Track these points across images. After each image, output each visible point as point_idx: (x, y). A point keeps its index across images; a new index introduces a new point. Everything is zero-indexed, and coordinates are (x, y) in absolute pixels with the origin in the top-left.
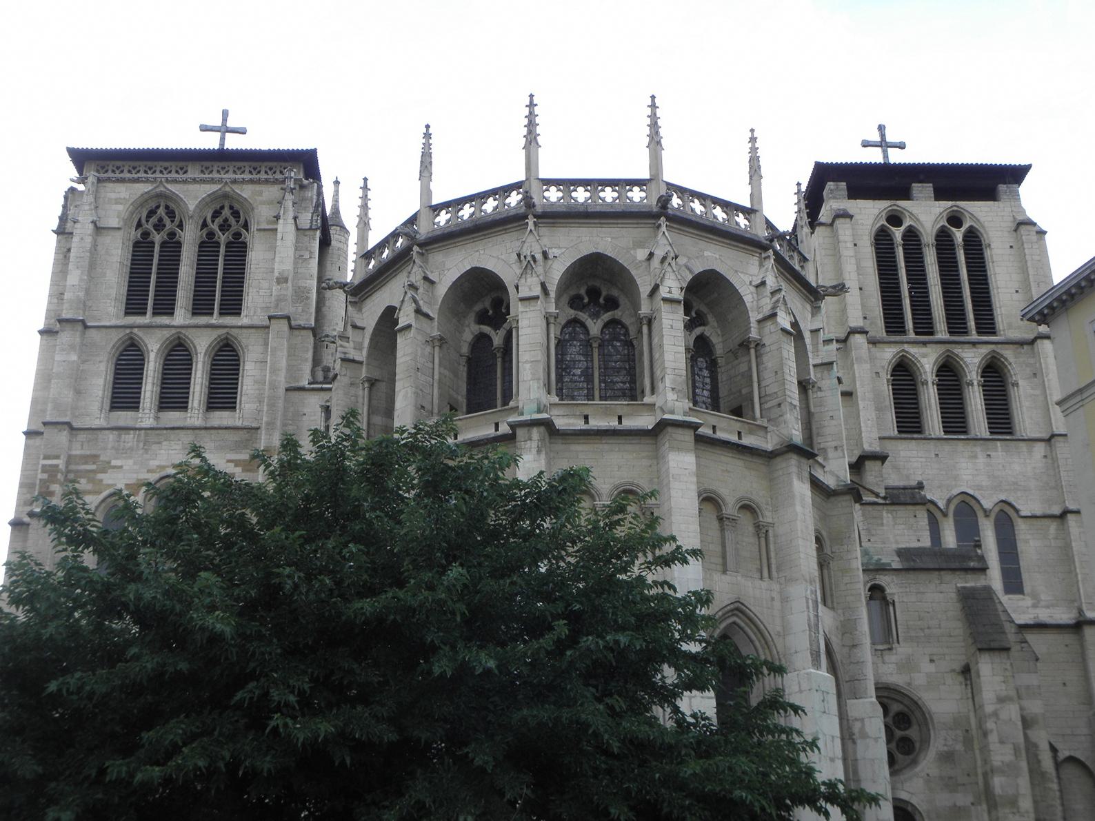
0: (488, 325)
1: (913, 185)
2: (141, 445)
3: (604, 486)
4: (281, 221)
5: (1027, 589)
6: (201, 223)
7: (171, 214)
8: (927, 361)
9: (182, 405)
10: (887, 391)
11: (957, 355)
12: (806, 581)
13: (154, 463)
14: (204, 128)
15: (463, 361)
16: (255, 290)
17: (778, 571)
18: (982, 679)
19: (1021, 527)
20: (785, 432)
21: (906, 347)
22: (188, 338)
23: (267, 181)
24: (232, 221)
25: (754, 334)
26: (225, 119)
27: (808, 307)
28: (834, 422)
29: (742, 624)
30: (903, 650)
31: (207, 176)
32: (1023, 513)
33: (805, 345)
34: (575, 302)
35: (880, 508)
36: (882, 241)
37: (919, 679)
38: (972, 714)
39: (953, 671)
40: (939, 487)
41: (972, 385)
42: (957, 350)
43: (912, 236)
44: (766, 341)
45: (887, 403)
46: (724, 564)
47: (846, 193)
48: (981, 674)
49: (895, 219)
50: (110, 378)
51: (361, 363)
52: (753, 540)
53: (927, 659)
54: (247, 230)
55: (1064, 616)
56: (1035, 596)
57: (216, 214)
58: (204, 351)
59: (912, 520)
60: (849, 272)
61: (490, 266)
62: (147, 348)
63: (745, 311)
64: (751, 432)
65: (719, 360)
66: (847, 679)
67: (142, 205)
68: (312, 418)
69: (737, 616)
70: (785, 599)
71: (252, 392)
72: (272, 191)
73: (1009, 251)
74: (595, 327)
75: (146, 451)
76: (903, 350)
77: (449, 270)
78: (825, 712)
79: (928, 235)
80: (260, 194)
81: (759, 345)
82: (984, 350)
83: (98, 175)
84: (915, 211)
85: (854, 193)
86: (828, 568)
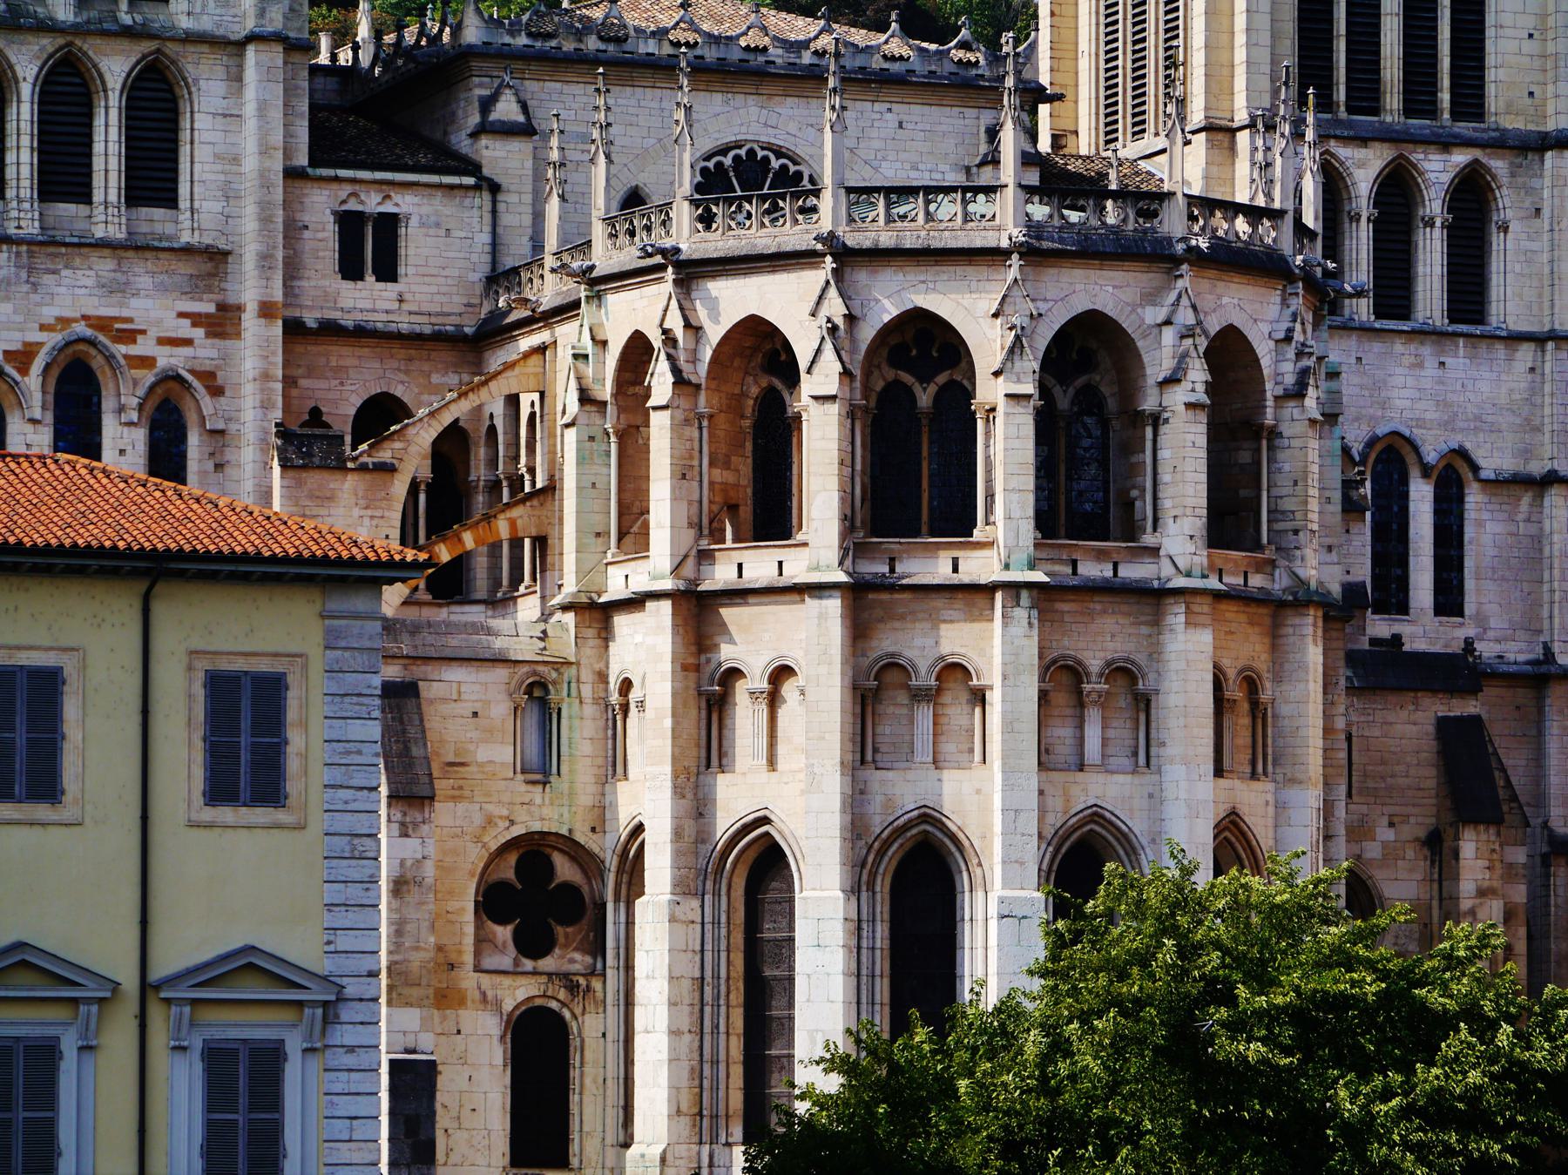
0: (908, 371)
2: (24, 275)
3: (1093, 662)
5: (1469, 608)
9: (83, 194)
11: (1415, 166)
13: (49, 313)
17: (1274, 765)
18: (1462, 863)
19: (1474, 498)
20: (1301, 572)
22: (85, 54)
25: (1269, 420)
29: (1233, 839)
32: (1484, 474)
38: (1435, 903)
39: (1417, 839)
41: (1432, 225)
42: (1417, 156)
44: (1286, 429)
48: (1461, 856)
51: (698, 387)
52: (1246, 721)
53: (1385, 821)
55: (1518, 652)
56: (1481, 620)
58: (118, 86)
62: (14, 72)
68: (320, 235)
70: (1280, 807)
71: (213, 177)
74: (1063, 401)
75: (35, 287)
81: (1274, 433)
82: (1460, 158)
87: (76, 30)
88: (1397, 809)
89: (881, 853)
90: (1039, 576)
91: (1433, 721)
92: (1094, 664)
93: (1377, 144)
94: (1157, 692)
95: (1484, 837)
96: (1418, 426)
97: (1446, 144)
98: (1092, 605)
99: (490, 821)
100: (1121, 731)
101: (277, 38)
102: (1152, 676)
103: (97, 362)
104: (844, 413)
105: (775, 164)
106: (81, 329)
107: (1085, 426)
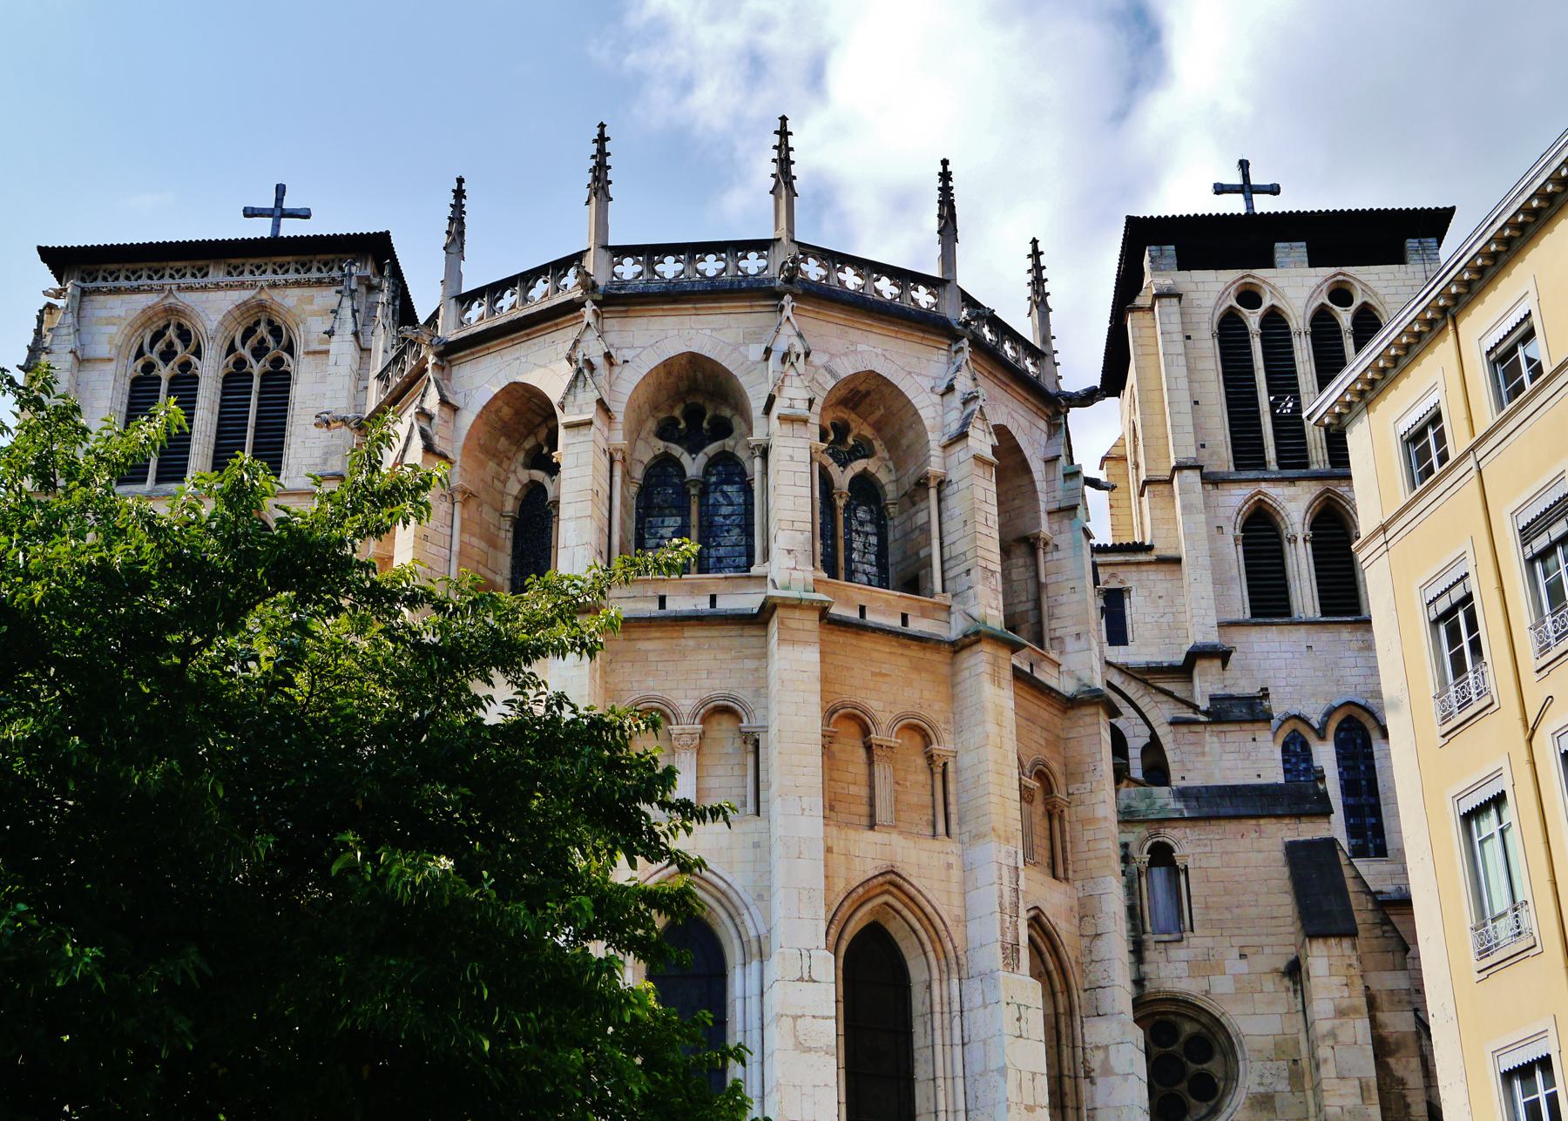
1: (1277, 245)
3: (683, 702)
4: (334, 338)
6: (226, 347)
7: (184, 335)
10: (1234, 556)
11: (1341, 497)
12: (999, 837)
14: (250, 213)
15: (506, 524)
16: (298, 441)
17: (960, 824)
20: (976, 612)
21: (1264, 487)
23: (319, 282)
26: (279, 199)
27: (1043, 425)
28: (1076, 597)
29: (899, 906)
30: (1197, 942)
31: (235, 278)
33: (1033, 482)
34: (666, 431)
35: (1200, 728)
36: (1230, 331)
37: (1222, 985)
38: (1302, 1037)
39: (1276, 970)
40: (1313, 695)
43: (1275, 322)
44: (953, 476)
45: (1235, 572)
46: (872, 816)
49: (1250, 297)
52: (923, 777)
53: (1235, 953)
54: (292, 355)
57: (248, 333)
59: (1250, 745)
60: (1176, 378)
61: (533, 379)
63: (922, 434)
64: (924, 613)
65: (891, 509)
66: (1086, 987)
67: (144, 326)
69: (890, 893)
70: (967, 869)
72: (328, 297)
74: (693, 466)
76: (1260, 492)
77: (477, 388)
78: (1021, 1036)
79: (1299, 319)
80: (311, 300)
83: (83, 285)
84: (1278, 283)
86: (1061, 819)
88: (1250, 941)
91: (1282, 848)
92: (686, 701)
93: (1304, 483)
94: (765, 729)
95: (1336, 951)
96: (1372, 697)
98: (683, 642)
102: (759, 713)
107: (724, 494)
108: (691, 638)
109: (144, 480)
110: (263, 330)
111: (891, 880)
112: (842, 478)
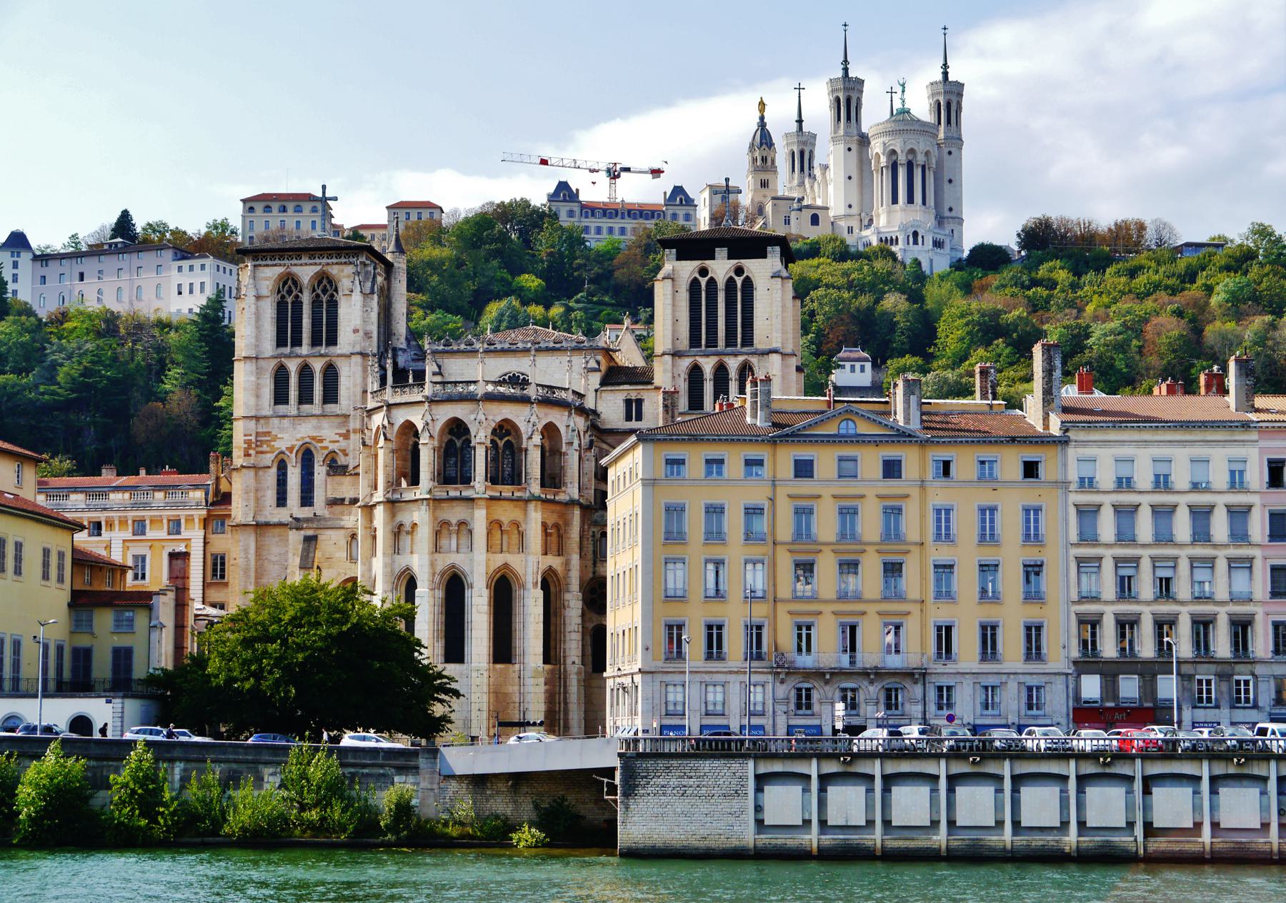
7: (295, 283)
8: (708, 365)
13: (299, 436)
21: (697, 358)
23: (345, 263)
24: (328, 286)
25: (524, 446)
26: (324, 193)
43: (712, 282)
47: (674, 256)
49: (704, 272)
50: (273, 387)
57: (320, 282)
64: (519, 490)
70: (526, 561)
72: (349, 269)
73: (767, 292)
74: (459, 443)
80: (343, 271)
81: (526, 450)
82: (741, 359)
85: (679, 258)
87: (308, 356)
89: (399, 579)
90: (428, 496)
92: (454, 521)
97: (736, 355)
99: (339, 574)
100: (464, 541)
101: (358, 353)
103: (312, 449)
104: (387, 451)
105: (521, 377)
106: (308, 440)
108: (455, 503)
109: (286, 345)
110: (325, 282)
111: (506, 565)
112: (501, 444)
